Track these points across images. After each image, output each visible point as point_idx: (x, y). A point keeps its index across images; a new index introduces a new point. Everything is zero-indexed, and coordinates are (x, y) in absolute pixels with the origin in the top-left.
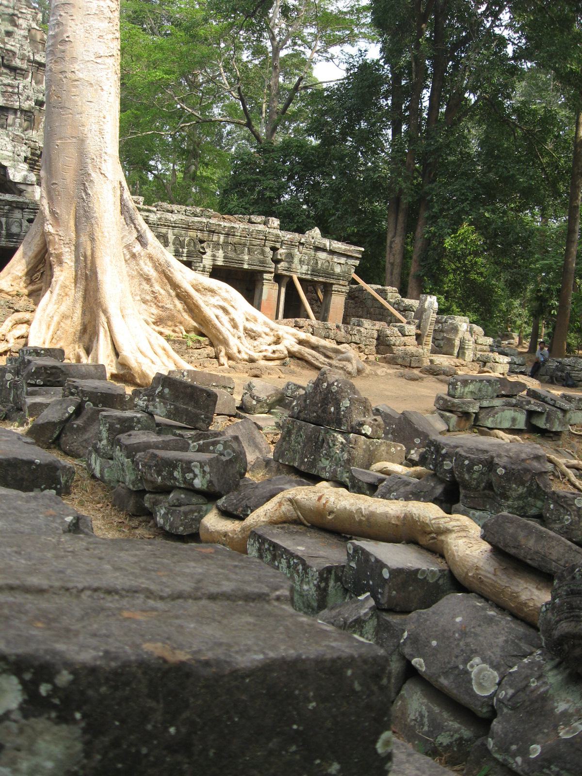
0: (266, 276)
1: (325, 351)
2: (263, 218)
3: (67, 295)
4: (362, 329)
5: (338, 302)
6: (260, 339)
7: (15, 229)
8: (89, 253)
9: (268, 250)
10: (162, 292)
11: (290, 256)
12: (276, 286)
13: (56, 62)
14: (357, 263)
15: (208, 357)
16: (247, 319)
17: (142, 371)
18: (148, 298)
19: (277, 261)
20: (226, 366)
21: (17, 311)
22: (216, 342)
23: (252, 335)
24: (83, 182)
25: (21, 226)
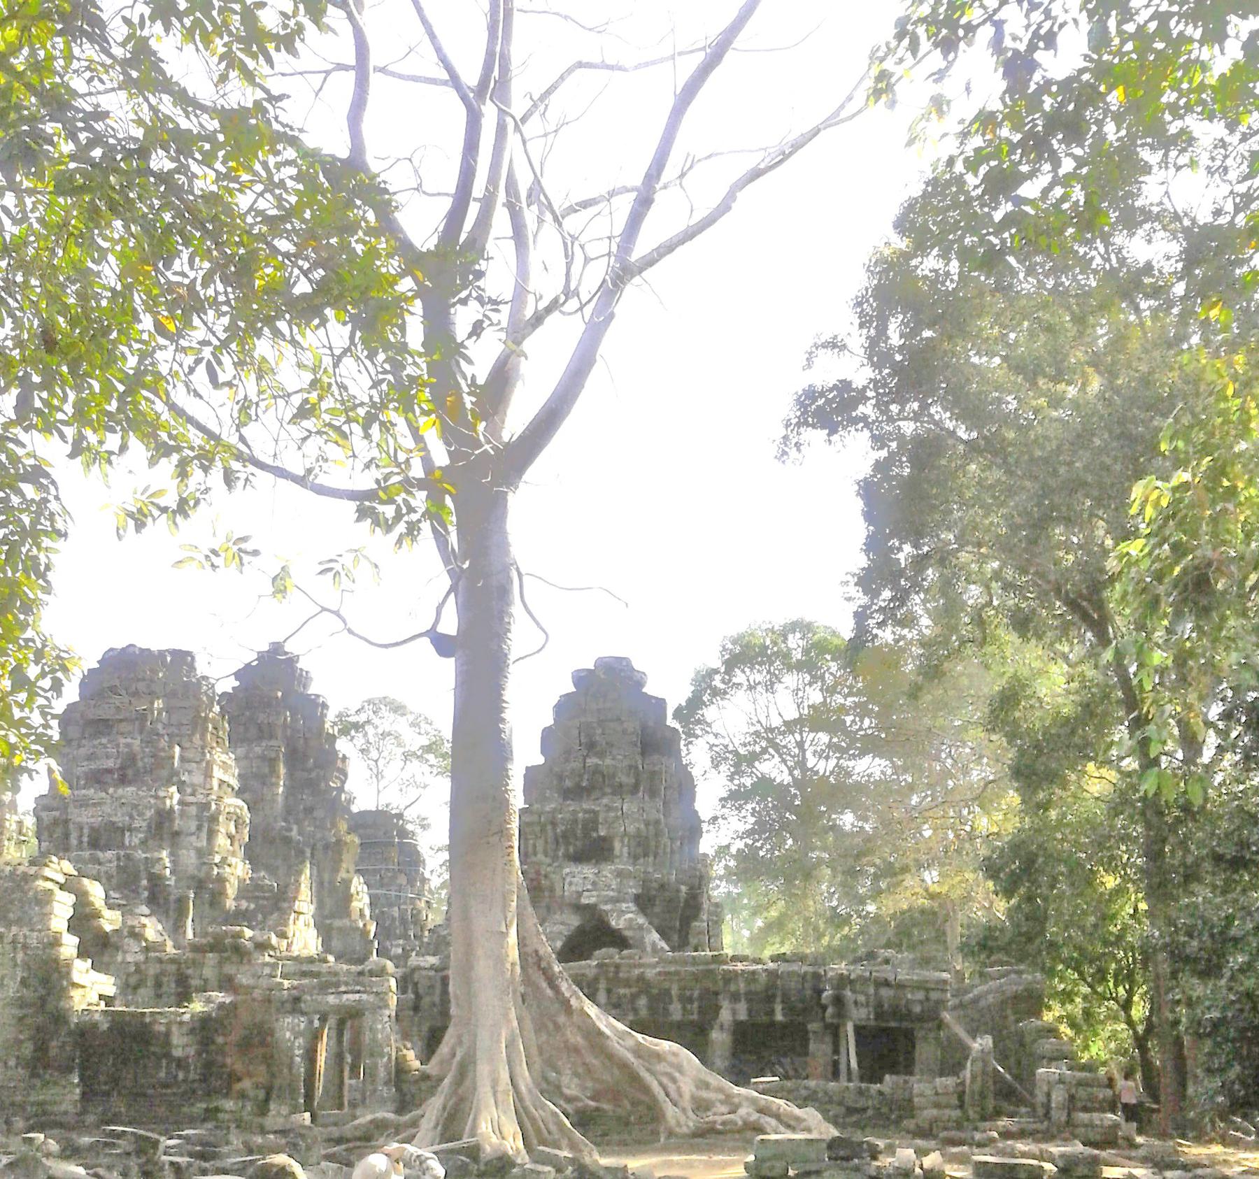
18: (580, 1070)
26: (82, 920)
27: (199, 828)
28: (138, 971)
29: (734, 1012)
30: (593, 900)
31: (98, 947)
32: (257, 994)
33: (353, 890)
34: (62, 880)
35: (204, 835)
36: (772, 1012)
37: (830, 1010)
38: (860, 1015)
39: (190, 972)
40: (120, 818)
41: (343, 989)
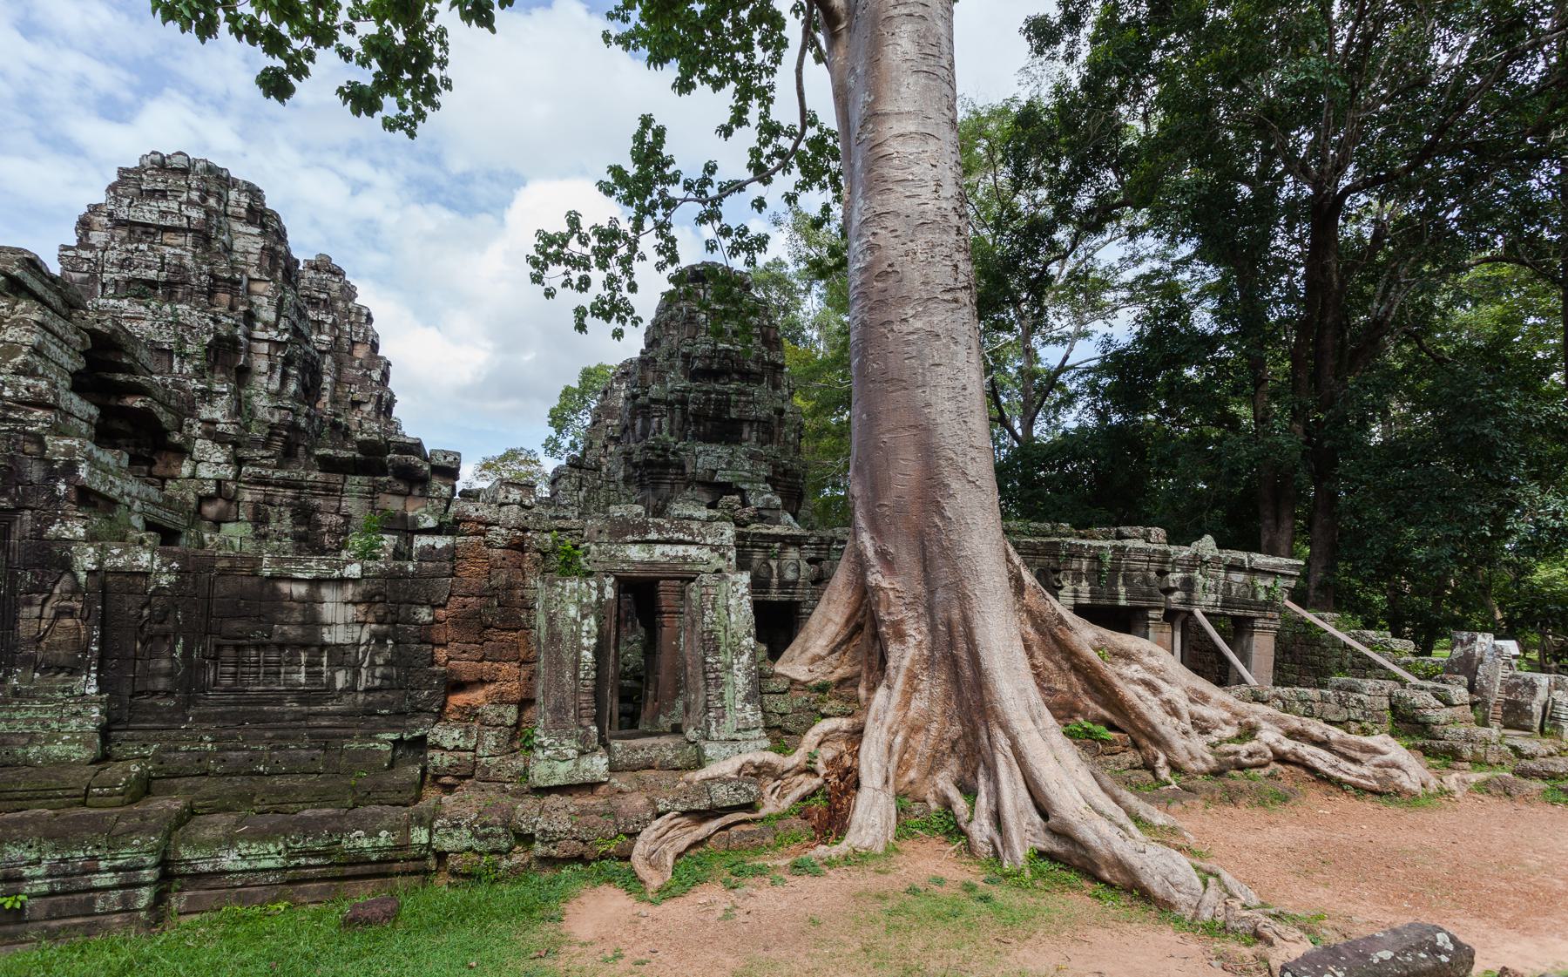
0: (1152, 614)
1: (1342, 749)
2: (1141, 529)
3: (915, 690)
4: (1362, 697)
5: (1263, 645)
6: (1218, 732)
7: (790, 575)
8: (956, 615)
10: (1050, 665)
11: (1188, 585)
12: (1168, 629)
13: (871, 309)
14: (1293, 583)
15: (1132, 767)
16: (1192, 700)
17: (1114, 855)
19: (1168, 591)
20: (1174, 785)
21: (824, 716)
22: (1144, 742)
23: (1202, 727)
24: (931, 492)
25: (799, 570)
27: (272, 368)
30: (728, 479)
32: (498, 534)
35: (277, 377)
36: (1115, 596)
37: (1178, 595)
39: (317, 502)
41: (653, 536)
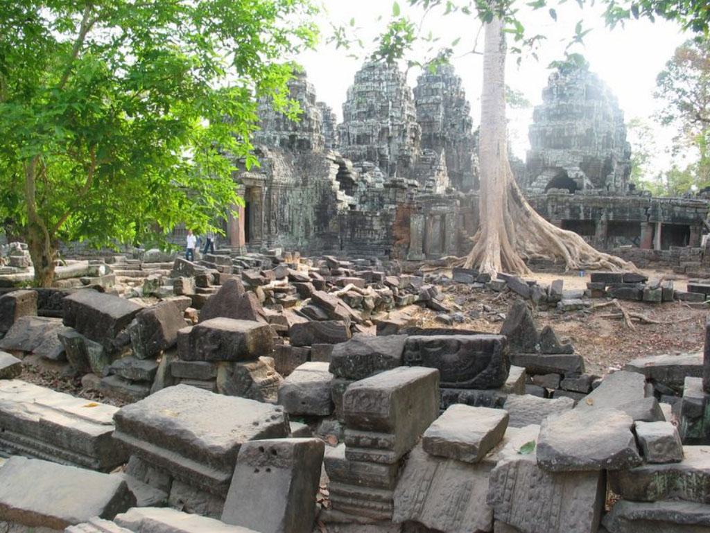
9: (641, 209)
16: (583, 249)
26: (343, 175)
27: (399, 135)
28: (365, 195)
29: (608, 216)
30: (561, 165)
31: (347, 184)
33: (472, 159)
34: (334, 158)
37: (651, 217)
38: (662, 220)
40: (368, 132)
